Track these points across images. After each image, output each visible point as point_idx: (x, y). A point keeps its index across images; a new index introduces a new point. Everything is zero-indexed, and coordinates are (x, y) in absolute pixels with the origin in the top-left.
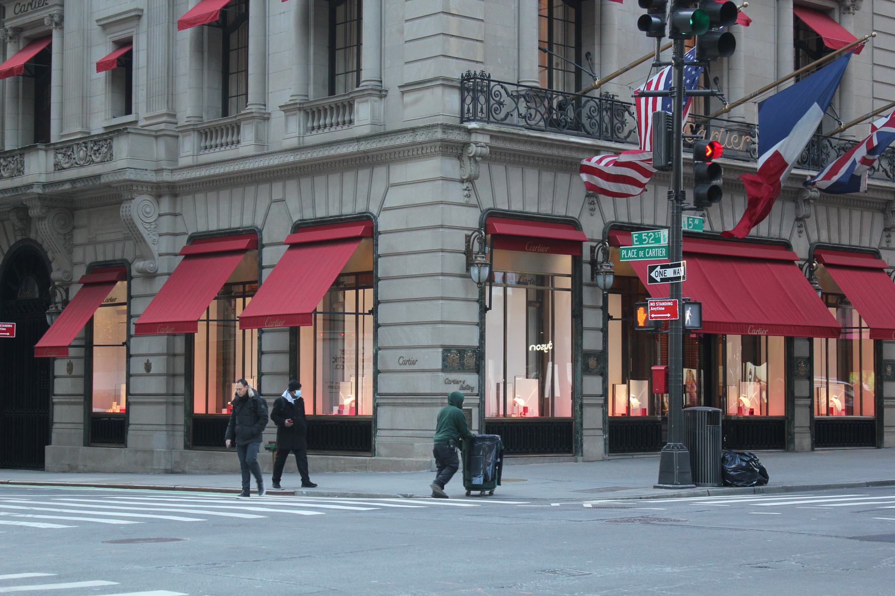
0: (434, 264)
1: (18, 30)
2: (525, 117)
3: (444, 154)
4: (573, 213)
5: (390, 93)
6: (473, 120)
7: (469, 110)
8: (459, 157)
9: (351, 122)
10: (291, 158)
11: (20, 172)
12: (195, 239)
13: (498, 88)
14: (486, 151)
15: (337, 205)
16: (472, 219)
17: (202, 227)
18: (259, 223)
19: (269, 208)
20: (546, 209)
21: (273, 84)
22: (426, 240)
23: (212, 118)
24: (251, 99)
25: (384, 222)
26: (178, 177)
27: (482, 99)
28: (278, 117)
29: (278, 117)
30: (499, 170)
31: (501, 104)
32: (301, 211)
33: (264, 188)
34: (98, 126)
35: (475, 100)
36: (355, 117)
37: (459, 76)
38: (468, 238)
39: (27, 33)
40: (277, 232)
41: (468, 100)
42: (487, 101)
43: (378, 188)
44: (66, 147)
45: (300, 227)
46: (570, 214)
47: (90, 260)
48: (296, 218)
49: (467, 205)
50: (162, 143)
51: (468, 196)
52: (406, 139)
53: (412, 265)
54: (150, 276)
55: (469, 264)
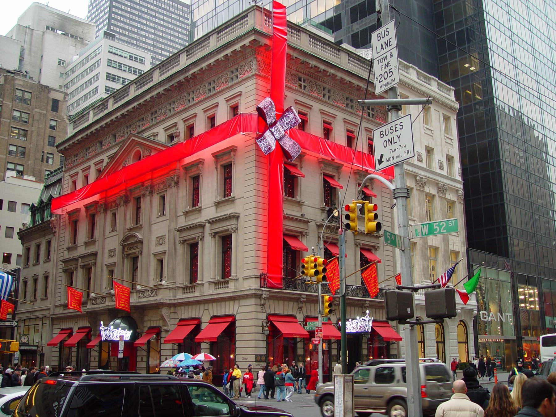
0: (253, 329)
1: (128, 255)
3: (255, 298)
4: (294, 314)
8: (260, 298)
12: (181, 320)
14: (268, 296)
16: (264, 316)
17: (183, 317)
21: (205, 274)
22: (250, 323)
23: (186, 283)
25: (237, 317)
26: (176, 301)
28: (206, 285)
29: (206, 285)
30: (272, 302)
33: (202, 306)
34: (151, 284)
36: (229, 285)
38: (263, 322)
40: (205, 319)
43: (236, 307)
44: (142, 292)
45: (213, 318)
47: (149, 326)
50: (171, 291)
53: (246, 330)
54: (167, 331)
55: (263, 330)
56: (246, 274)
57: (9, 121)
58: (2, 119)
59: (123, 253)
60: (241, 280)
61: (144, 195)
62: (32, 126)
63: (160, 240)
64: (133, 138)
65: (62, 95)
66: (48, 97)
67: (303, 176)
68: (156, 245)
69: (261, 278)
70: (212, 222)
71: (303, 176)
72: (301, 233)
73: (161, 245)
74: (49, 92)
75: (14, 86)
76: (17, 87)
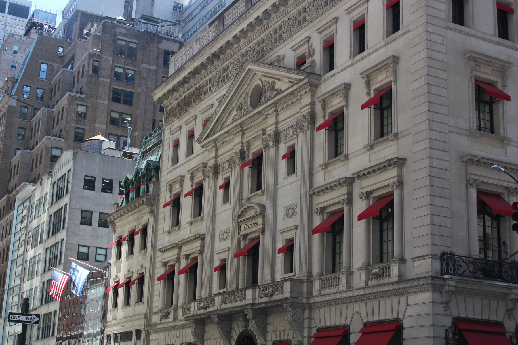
2: (472, 273)
5: (408, 262)
6: (448, 274)
7: (444, 269)
8: (441, 292)
9: (389, 275)
10: (362, 292)
11: (244, 299)
13: (459, 259)
15: (384, 314)
16: (448, 322)
17: (323, 325)
18: (348, 323)
19: (353, 316)
20: (485, 317)
24: (344, 265)
25: (406, 323)
27: (451, 264)
31: (460, 266)
32: (367, 317)
34: (279, 277)
35: (447, 264)
37: (439, 253)
38: (446, 331)
39: (250, 237)
41: (444, 265)
42: (454, 265)
44: (265, 287)
46: (498, 320)
47: (274, 339)
48: (365, 320)
49: (445, 315)
51: (446, 311)
52: (415, 283)
56: (418, 253)
57: (109, 80)
58: (101, 79)
59: (239, 234)
60: (409, 263)
61: (266, 147)
62: (139, 86)
63: (289, 212)
64: (250, 67)
65: (177, 45)
66: (158, 49)
67: (508, 98)
68: (284, 218)
69: (442, 260)
70: (362, 175)
71: (508, 98)
72: (507, 188)
73: (290, 217)
74: (160, 42)
75: (115, 35)
76: (118, 37)
